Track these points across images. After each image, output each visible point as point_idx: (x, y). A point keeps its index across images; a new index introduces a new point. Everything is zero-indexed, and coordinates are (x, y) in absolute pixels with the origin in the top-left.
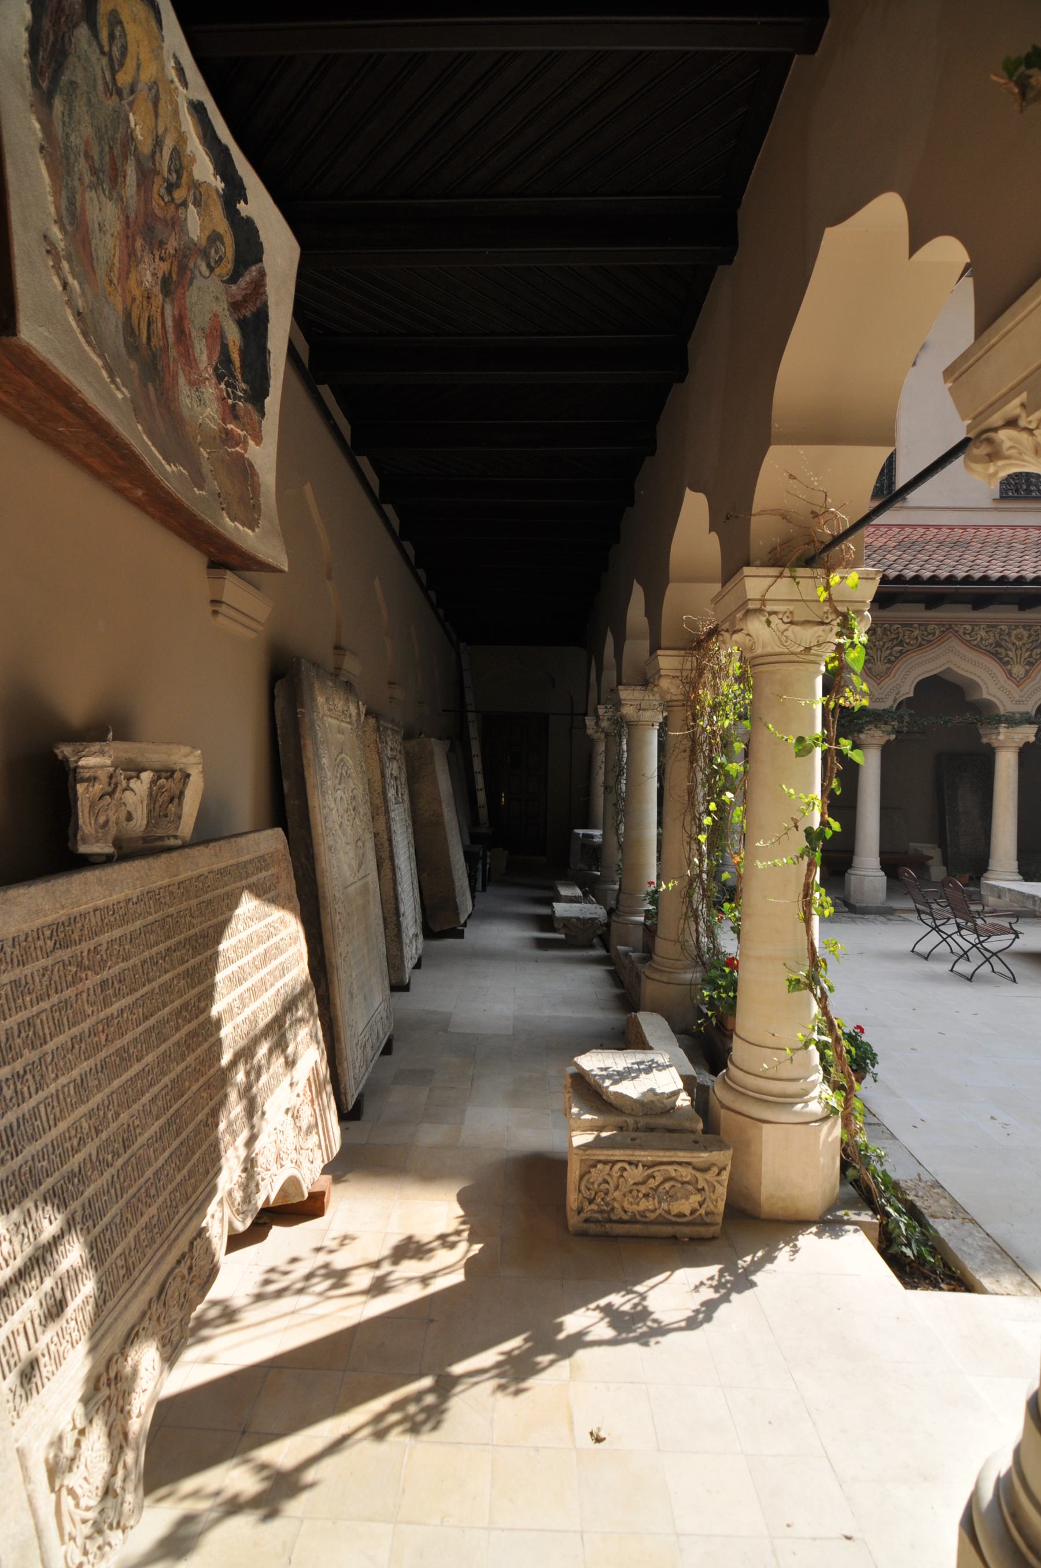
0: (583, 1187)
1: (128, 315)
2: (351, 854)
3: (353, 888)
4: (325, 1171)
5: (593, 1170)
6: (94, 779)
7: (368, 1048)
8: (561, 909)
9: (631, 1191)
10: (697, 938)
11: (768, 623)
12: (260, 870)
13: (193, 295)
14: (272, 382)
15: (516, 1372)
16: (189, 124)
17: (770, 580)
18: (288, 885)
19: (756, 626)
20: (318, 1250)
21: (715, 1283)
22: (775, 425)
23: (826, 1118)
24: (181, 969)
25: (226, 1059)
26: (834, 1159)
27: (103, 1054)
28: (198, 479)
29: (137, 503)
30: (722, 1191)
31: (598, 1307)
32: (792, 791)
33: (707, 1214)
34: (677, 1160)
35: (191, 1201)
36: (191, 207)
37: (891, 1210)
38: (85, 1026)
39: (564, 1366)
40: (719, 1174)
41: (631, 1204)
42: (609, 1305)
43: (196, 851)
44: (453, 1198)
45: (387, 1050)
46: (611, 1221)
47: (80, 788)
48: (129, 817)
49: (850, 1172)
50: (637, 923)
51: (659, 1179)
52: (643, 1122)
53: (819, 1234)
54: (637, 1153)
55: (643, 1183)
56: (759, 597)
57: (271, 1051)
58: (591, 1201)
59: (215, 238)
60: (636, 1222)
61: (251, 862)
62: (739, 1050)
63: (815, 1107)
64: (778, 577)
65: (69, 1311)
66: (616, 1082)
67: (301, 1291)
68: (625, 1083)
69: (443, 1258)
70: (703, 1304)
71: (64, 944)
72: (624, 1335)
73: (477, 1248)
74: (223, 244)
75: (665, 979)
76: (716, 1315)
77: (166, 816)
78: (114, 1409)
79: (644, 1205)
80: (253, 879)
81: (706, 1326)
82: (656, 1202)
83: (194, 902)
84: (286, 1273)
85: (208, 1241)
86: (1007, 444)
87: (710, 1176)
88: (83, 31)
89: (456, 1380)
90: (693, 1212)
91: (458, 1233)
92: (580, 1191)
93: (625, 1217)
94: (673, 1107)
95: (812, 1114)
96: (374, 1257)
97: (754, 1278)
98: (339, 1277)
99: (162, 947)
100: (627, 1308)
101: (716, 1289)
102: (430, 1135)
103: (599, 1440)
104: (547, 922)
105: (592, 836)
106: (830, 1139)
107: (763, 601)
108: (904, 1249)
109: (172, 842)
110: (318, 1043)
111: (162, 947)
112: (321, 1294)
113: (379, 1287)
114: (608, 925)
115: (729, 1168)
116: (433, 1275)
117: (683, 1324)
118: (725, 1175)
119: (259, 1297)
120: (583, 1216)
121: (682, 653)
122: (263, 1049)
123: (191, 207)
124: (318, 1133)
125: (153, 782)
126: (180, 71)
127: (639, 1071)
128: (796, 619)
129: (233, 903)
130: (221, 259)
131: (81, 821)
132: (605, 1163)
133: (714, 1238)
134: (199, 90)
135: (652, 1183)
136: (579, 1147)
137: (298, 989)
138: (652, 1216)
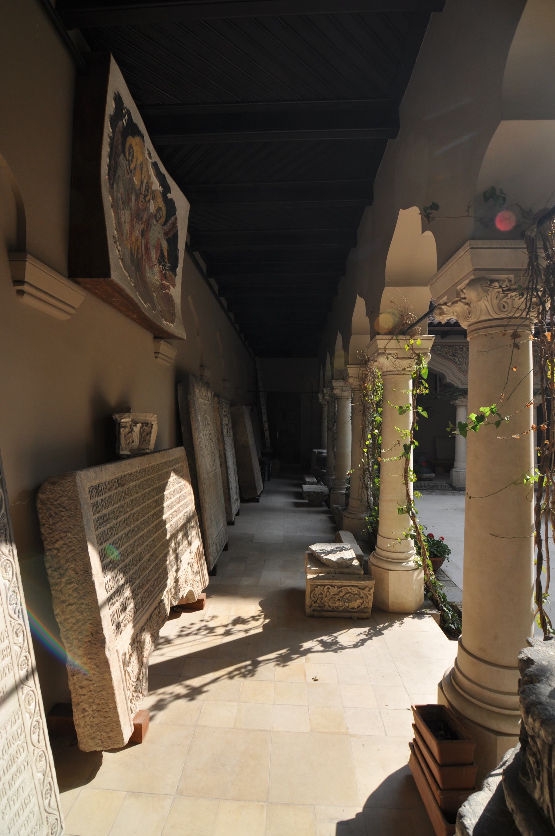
0: (312, 596)
1: (131, 249)
2: (210, 459)
3: (211, 474)
4: (203, 592)
6: (125, 427)
7: (218, 546)
8: (306, 488)
9: (332, 598)
10: (368, 497)
11: (387, 358)
12: (176, 463)
13: (151, 234)
14: (179, 261)
15: (283, 660)
16: (152, 172)
17: (387, 341)
18: (187, 471)
19: (382, 360)
20: (202, 621)
21: (366, 633)
22: (387, 279)
23: (417, 569)
24: (153, 499)
25: (168, 537)
26: (421, 587)
27: (132, 526)
28: (154, 307)
29: (133, 320)
30: (371, 598)
31: (317, 640)
32: (399, 429)
33: (365, 608)
35: (159, 586)
36: (152, 201)
37: (445, 609)
38: (127, 515)
39: (303, 658)
40: (369, 591)
42: (322, 640)
43: (156, 455)
44: (257, 604)
45: (226, 549)
46: (324, 611)
47: (122, 430)
50: (342, 494)
51: (344, 593)
52: (338, 570)
53: (413, 618)
54: (335, 581)
55: (337, 594)
56: (383, 347)
57: (183, 537)
58: (315, 602)
59: (159, 209)
60: (335, 611)
61: (173, 460)
62: (380, 541)
63: (412, 564)
64: (391, 339)
66: (326, 555)
67: (196, 634)
68: (330, 555)
69: (253, 624)
70: (360, 640)
71: (120, 486)
73: (267, 621)
74: (162, 211)
75: (353, 517)
76: (366, 644)
77: (145, 441)
79: (338, 604)
80: (174, 467)
81: (361, 647)
83: (156, 474)
84: (189, 628)
85: (164, 605)
86: (445, 310)
87: (366, 591)
88: (122, 156)
89: (260, 662)
90: (359, 607)
91: (259, 616)
92: (310, 598)
93: (330, 609)
94: (351, 565)
95: (410, 567)
96: (226, 623)
97: (383, 632)
98: (211, 630)
99: (147, 490)
100: (329, 641)
101: (367, 635)
102: (247, 581)
103: (316, 680)
104: (300, 495)
105: (322, 453)
106: (418, 578)
107: (385, 349)
108: (451, 625)
109: (148, 451)
111: (147, 490)
112: (204, 635)
113: (228, 633)
115: (373, 588)
116: (250, 629)
118: (372, 591)
119: (179, 636)
120: (312, 608)
121: (359, 366)
122: (180, 536)
123: (152, 201)
125: (141, 428)
126: (149, 154)
127: (337, 551)
128: (399, 357)
130: (161, 217)
132: (321, 586)
133: (367, 618)
134: (156, 158)
135: (341, 594)
136: (310, 579)
137: (191, 514)
138: (341, 609)
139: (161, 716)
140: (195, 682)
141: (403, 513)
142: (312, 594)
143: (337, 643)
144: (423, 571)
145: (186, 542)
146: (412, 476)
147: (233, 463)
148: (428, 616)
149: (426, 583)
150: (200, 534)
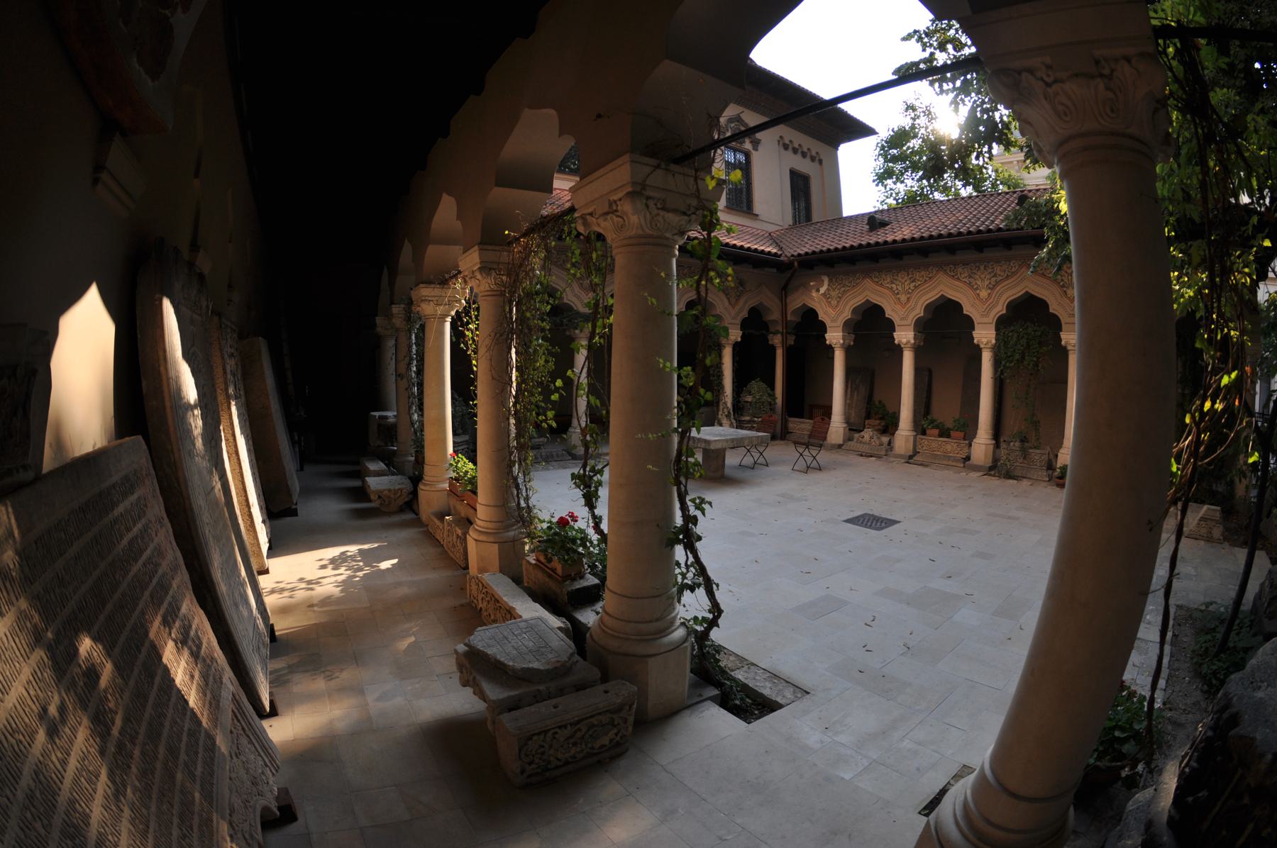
58: (530, 764)
90: (611, 741)
93: (559, 763)
105: (386, 417)
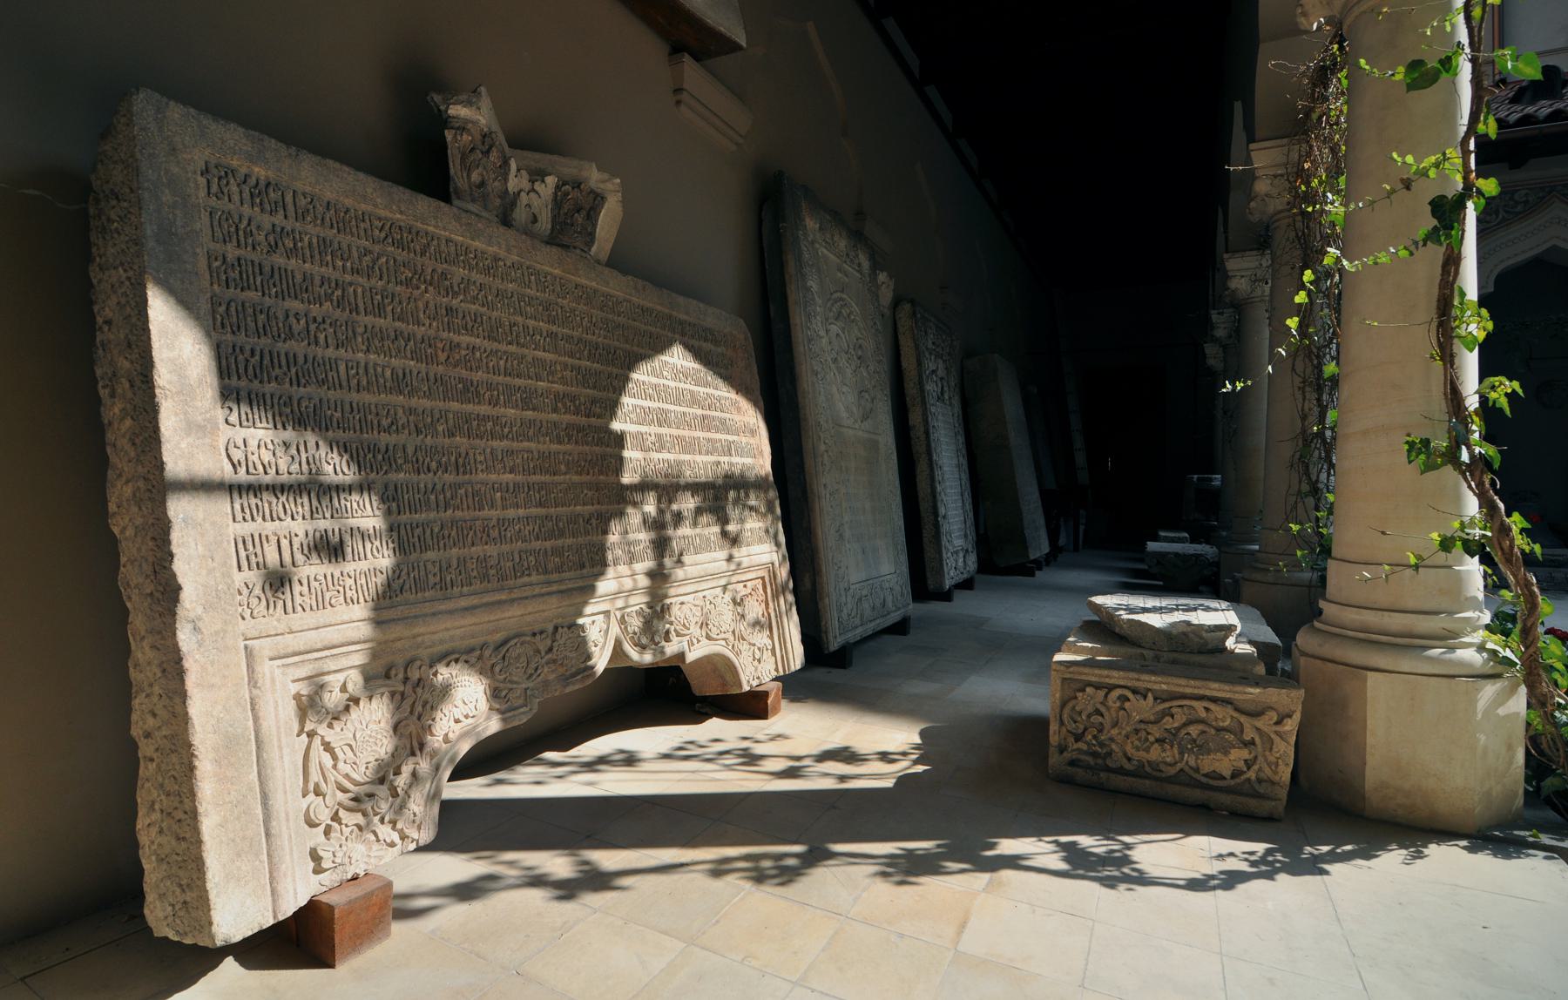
0: (1065, 716)
4: (776, 679)
5: (1079, 695)
6: (463, 129)
7: (866, 605)
9: (1137, 731)
15: (909, 868)
18: (756, 385)
20: (745, 738)
21: (1253, 858)
25: (627, 479)
26: (1510, 748)
30: (1285, 750)
32: (1410, 159)
33: (1260, 781)
34: (1208, 693)
40: (1278, 723)
41: (1138, 749)
42: (1074, 843)
47: (449, 135)
48: (535, 220)
49: (1550, 783)
51: (1180, 719)
53: (1471, 849)
54: (1145, 677)
57: (699, 511)
58: (1078, 738)
60: (1147, 776)
65: (350, 567)
70: (1222, 873)
71: (400, 244)
72: (1081, 872)
73: (920, 768)
76: (1241, 887)
78: (407, 705)
79: (1155, 754)
80: (695, 343)
81: (1219, 892)
82: (1176, 751)
90: (1236, 774)
91: (904, 754)
93: (1128, 766)
95: (1461, 663)
97: (1326, 867)
98: (750, 759)
101: (1253, 864)
106: (1501, 711)
110: (778, 544)
114: (1217, 564)
115: (1297, 717)
117: (1182, 883)
118: (1291, 726)
119: (666, 756)
121: (1285, 141)
122: (687, 503)
124: (771, 637)
125: (558, 188)
129: (660, 347)
131: (452, 172)
132: (1097, 687)
133: (1270, 819)
135: (1168, 723)
138: (1172, 771)
139: (456, 913)
140: (607, 859)
141: (1429, 467)
142: (1066, 711)
143: (1126, 861)
144: (1523, 690)
145: (716, 529)
146: (1476, 327)
147: (959, 466)
148: (1542, 854)
149: (1533, 740)
150: (782, 538)
